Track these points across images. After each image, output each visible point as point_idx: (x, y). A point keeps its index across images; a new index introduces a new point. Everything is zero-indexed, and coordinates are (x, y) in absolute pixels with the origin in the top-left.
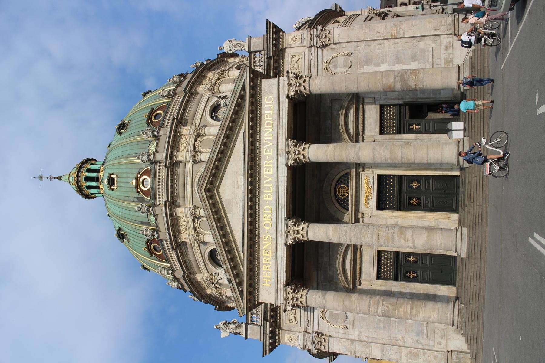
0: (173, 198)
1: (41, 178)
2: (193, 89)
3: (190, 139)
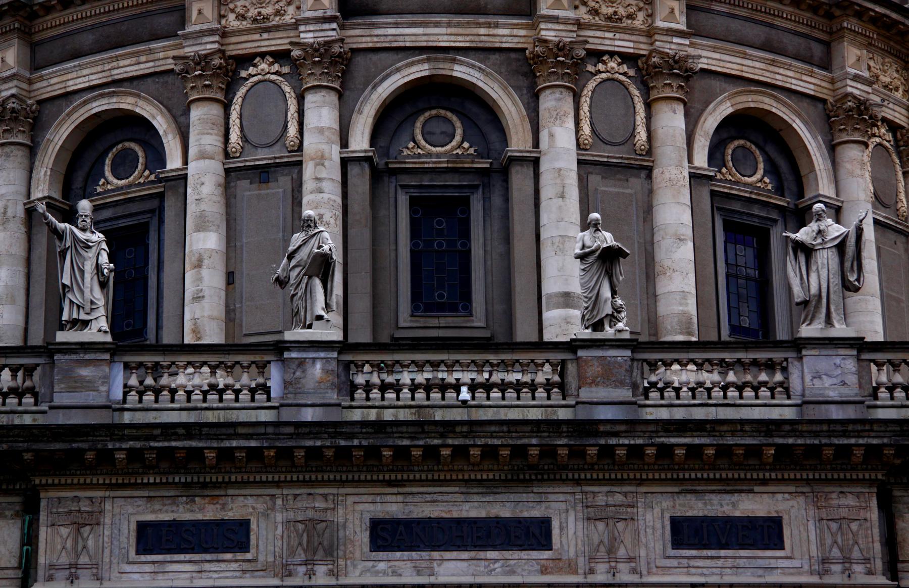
2: (854, 21)
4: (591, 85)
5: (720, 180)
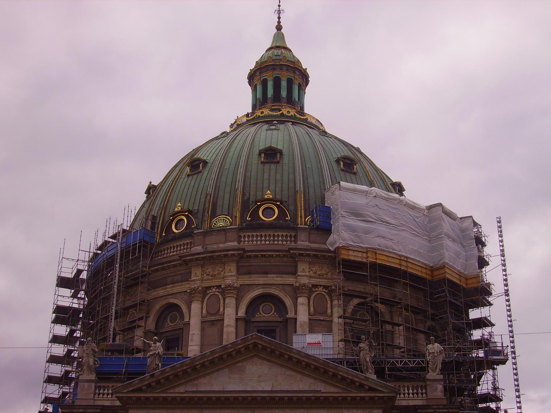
0: (250, 257)
3: (328, 279)
4: (313, 295)
5: (356, 324)
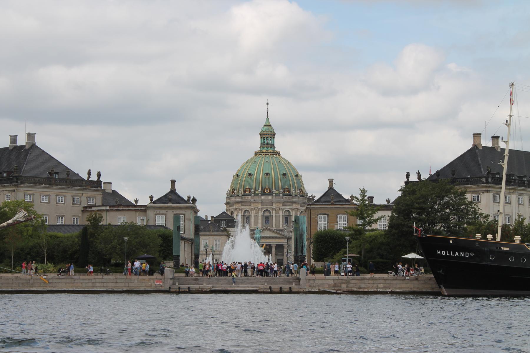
1: (268, 104)
